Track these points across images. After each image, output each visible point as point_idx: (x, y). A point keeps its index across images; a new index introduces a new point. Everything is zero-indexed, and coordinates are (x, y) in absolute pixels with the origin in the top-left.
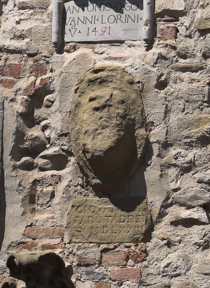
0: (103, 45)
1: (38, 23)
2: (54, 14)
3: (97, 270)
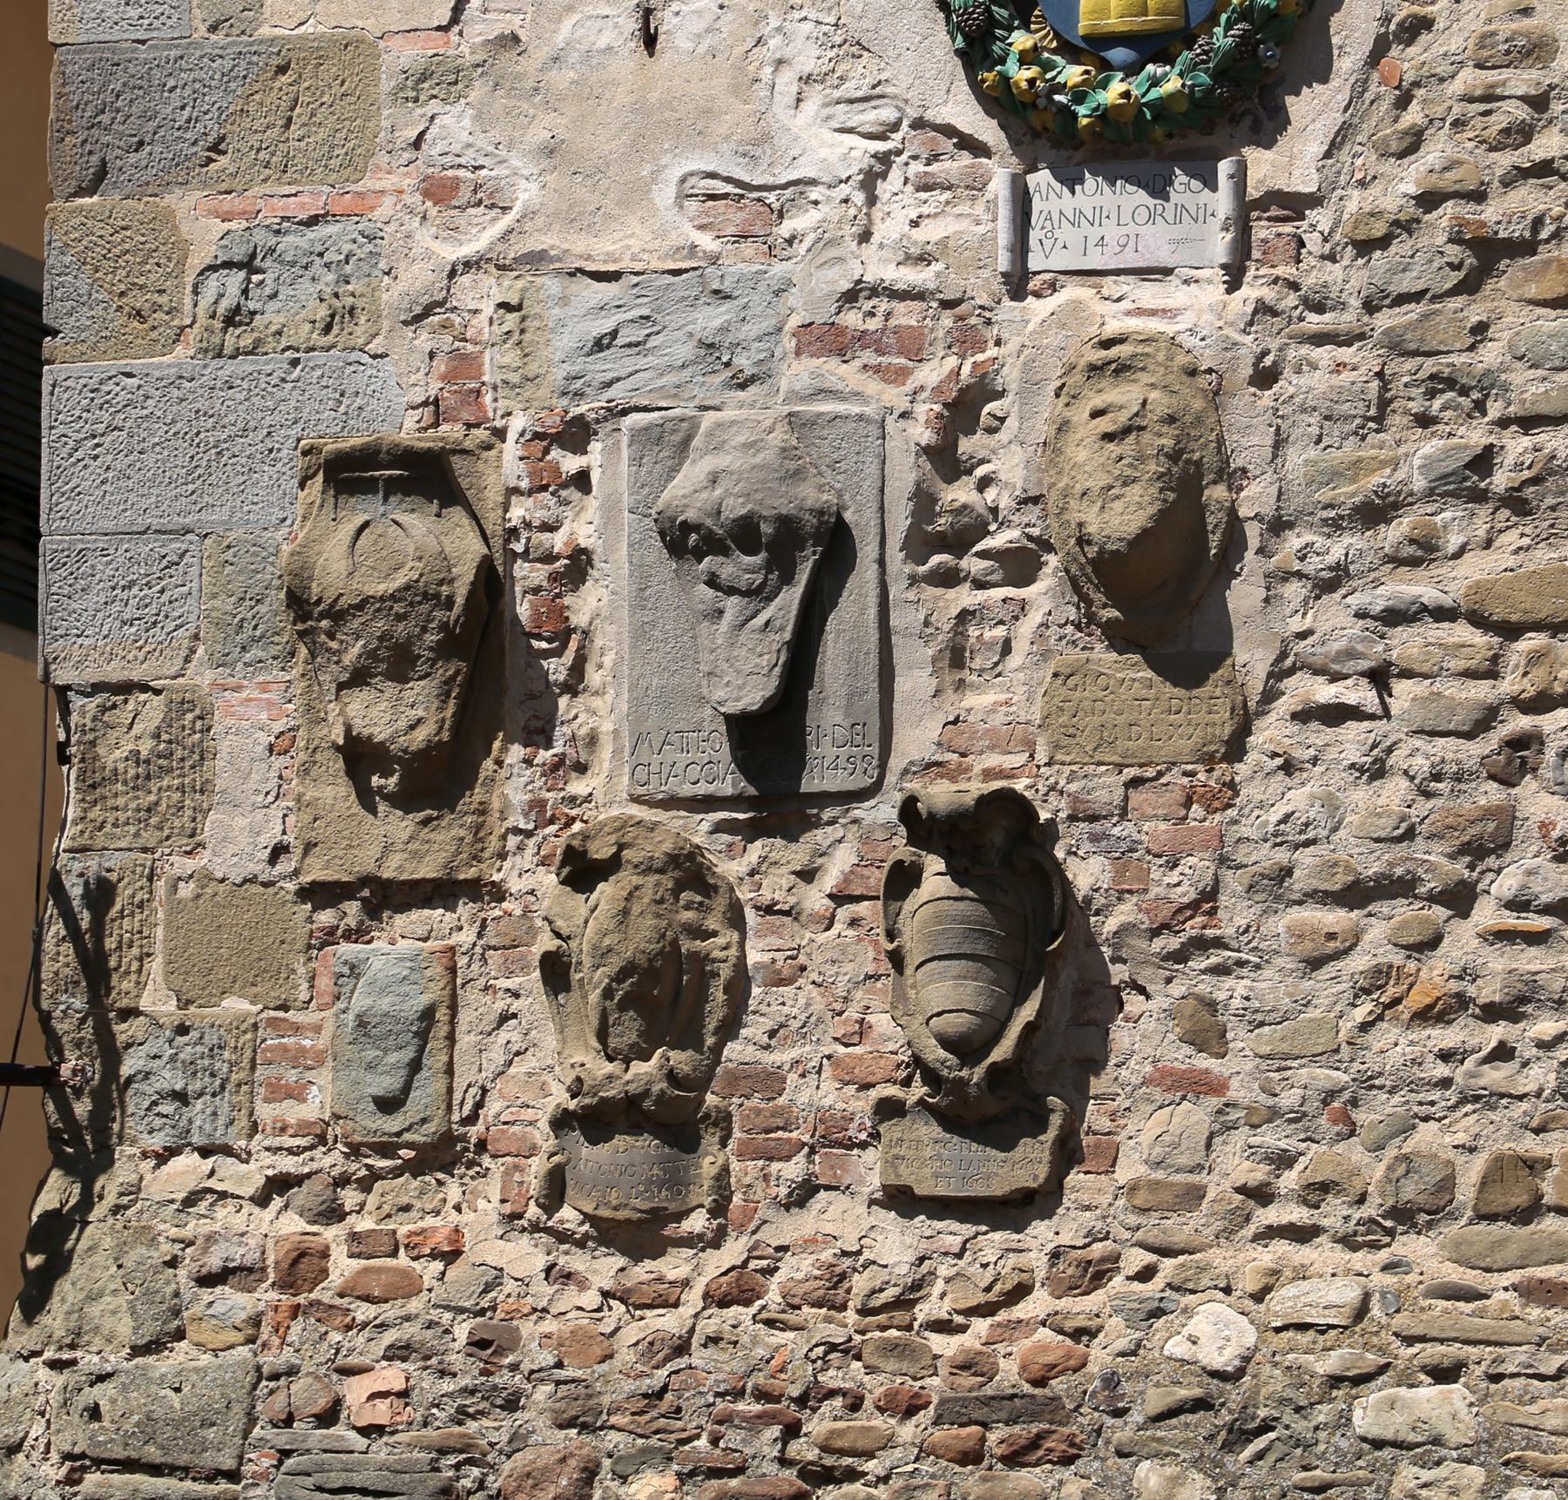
0: (1122, 278)
1: (964, 225)
2: (1001, 204)
3: (1116, 831)
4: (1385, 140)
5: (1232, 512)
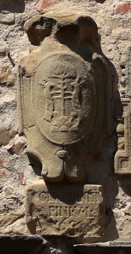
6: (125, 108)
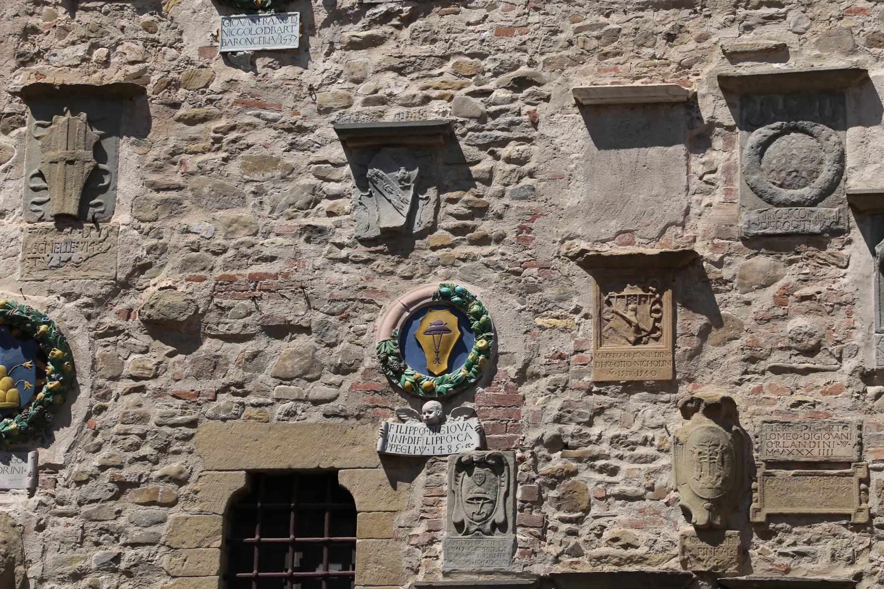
4: (89, 447)
5: (25, 576)
6: (758, 470)
